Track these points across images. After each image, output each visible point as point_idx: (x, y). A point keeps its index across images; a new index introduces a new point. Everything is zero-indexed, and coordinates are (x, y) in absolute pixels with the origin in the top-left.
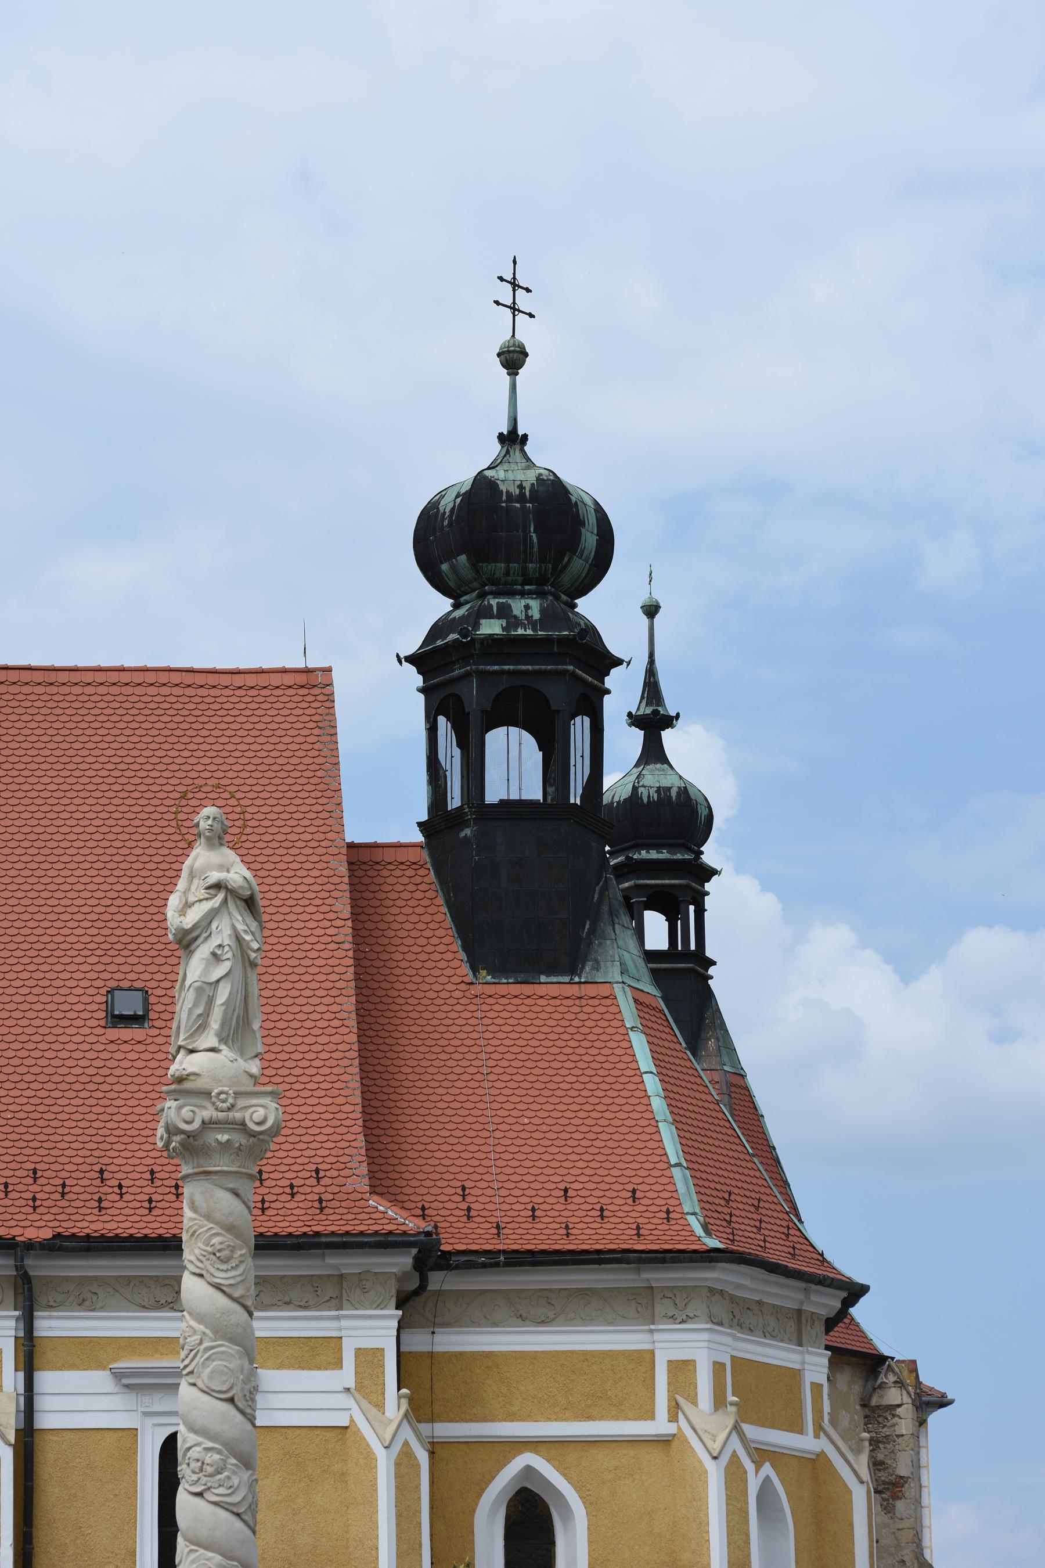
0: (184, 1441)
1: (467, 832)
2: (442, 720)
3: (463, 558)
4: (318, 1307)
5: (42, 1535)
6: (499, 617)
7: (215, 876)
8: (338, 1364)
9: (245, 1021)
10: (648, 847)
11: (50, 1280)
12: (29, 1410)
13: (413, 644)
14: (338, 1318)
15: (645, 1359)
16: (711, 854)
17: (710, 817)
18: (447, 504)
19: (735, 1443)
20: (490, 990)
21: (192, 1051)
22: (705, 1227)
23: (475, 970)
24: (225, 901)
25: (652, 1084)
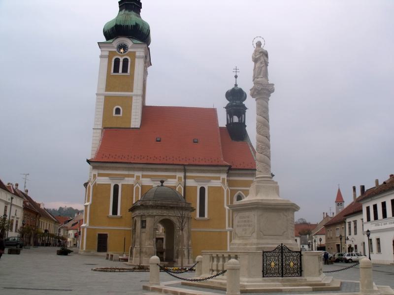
11: (188, 170)
13: (225, 106)
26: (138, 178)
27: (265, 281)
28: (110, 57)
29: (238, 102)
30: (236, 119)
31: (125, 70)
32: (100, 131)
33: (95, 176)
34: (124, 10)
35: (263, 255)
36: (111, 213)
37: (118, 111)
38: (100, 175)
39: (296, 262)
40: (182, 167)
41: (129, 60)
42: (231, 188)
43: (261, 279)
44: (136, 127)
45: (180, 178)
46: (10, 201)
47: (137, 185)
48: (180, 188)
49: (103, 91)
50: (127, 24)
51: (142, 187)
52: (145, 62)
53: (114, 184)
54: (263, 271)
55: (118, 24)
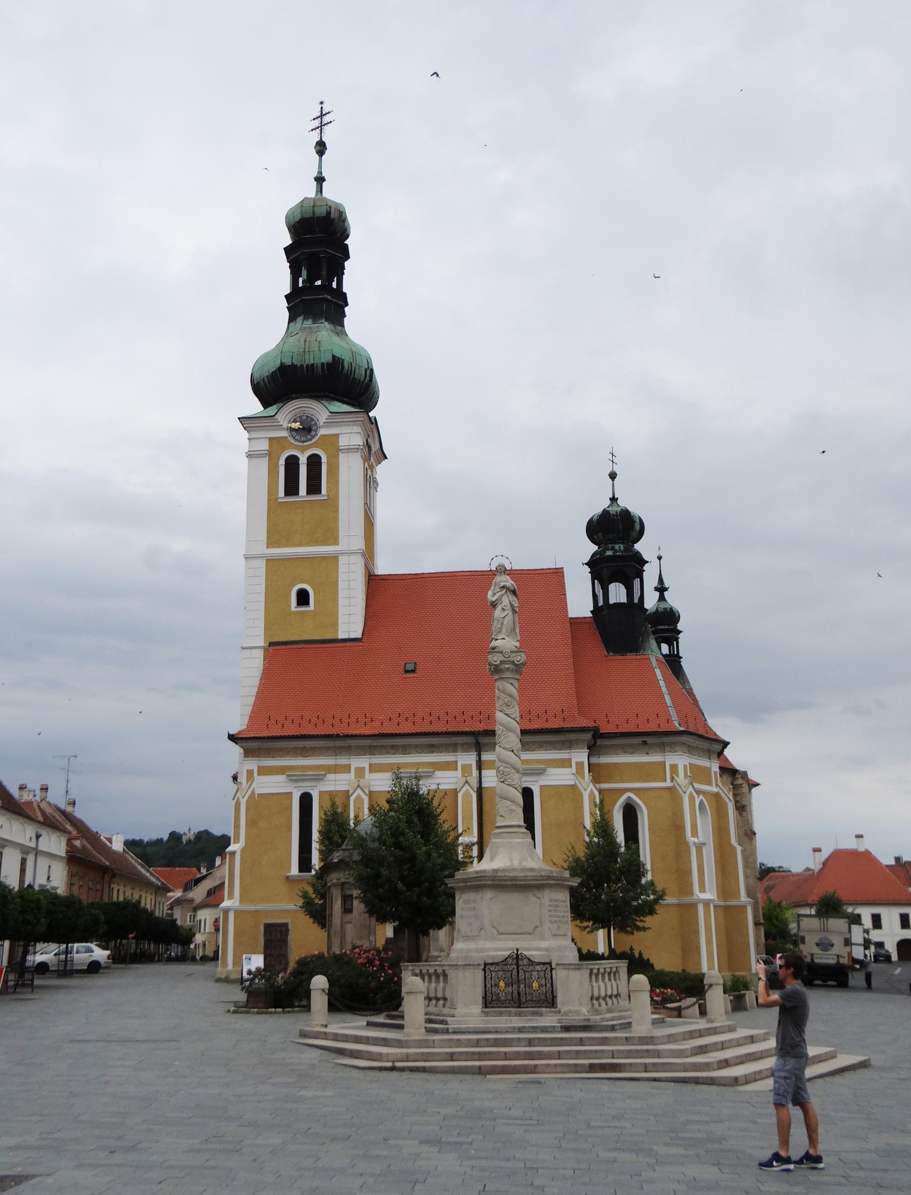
0: (498, 764)
1: (605, 612)
2: (596, 581)
3: (600, 534)
4: (564, 749)
5: (485, 817)
6: (612, 550)
7: (502, 584)
8: (571, 766)
9: (514, 629)
10: (662, 625)
12: (480, 782)
14: (570, 753)
15: (663, 764)
16: (680, 626)
17: (679, 616)
18: (595, 518)
19: (691, 788)
20: (613, 658)
21: (497, 640)
22: (680, 725)
23: (608, 652)
24: (506, 591)
25: (662, 683)
26: (360, 772)
27: (487, 1014)
28: (272, 456)
29: (620, 547)
30: (617, 593)
31: (314, 487)
32: (260, 654)
33: (250, 773)
34: (300, 319)
35: (484, 970)
36: (294, 870)
37: (303, 598)
38: (263, 771)
39: (543, 981)
40: (470, 740)
41: (324, 459)
42: (604, 786)
43: (477, 1009)
44: (353, 636)
45: (466, 768)
46: (33, 845)
47: (359, 791)
48: (467, 794)
49: (262, 548)
50: (310, 360)
51: (371, 795)
52: (366, 459)
53: (301, 792)
54: (485, 998)
55: (288, 362)
